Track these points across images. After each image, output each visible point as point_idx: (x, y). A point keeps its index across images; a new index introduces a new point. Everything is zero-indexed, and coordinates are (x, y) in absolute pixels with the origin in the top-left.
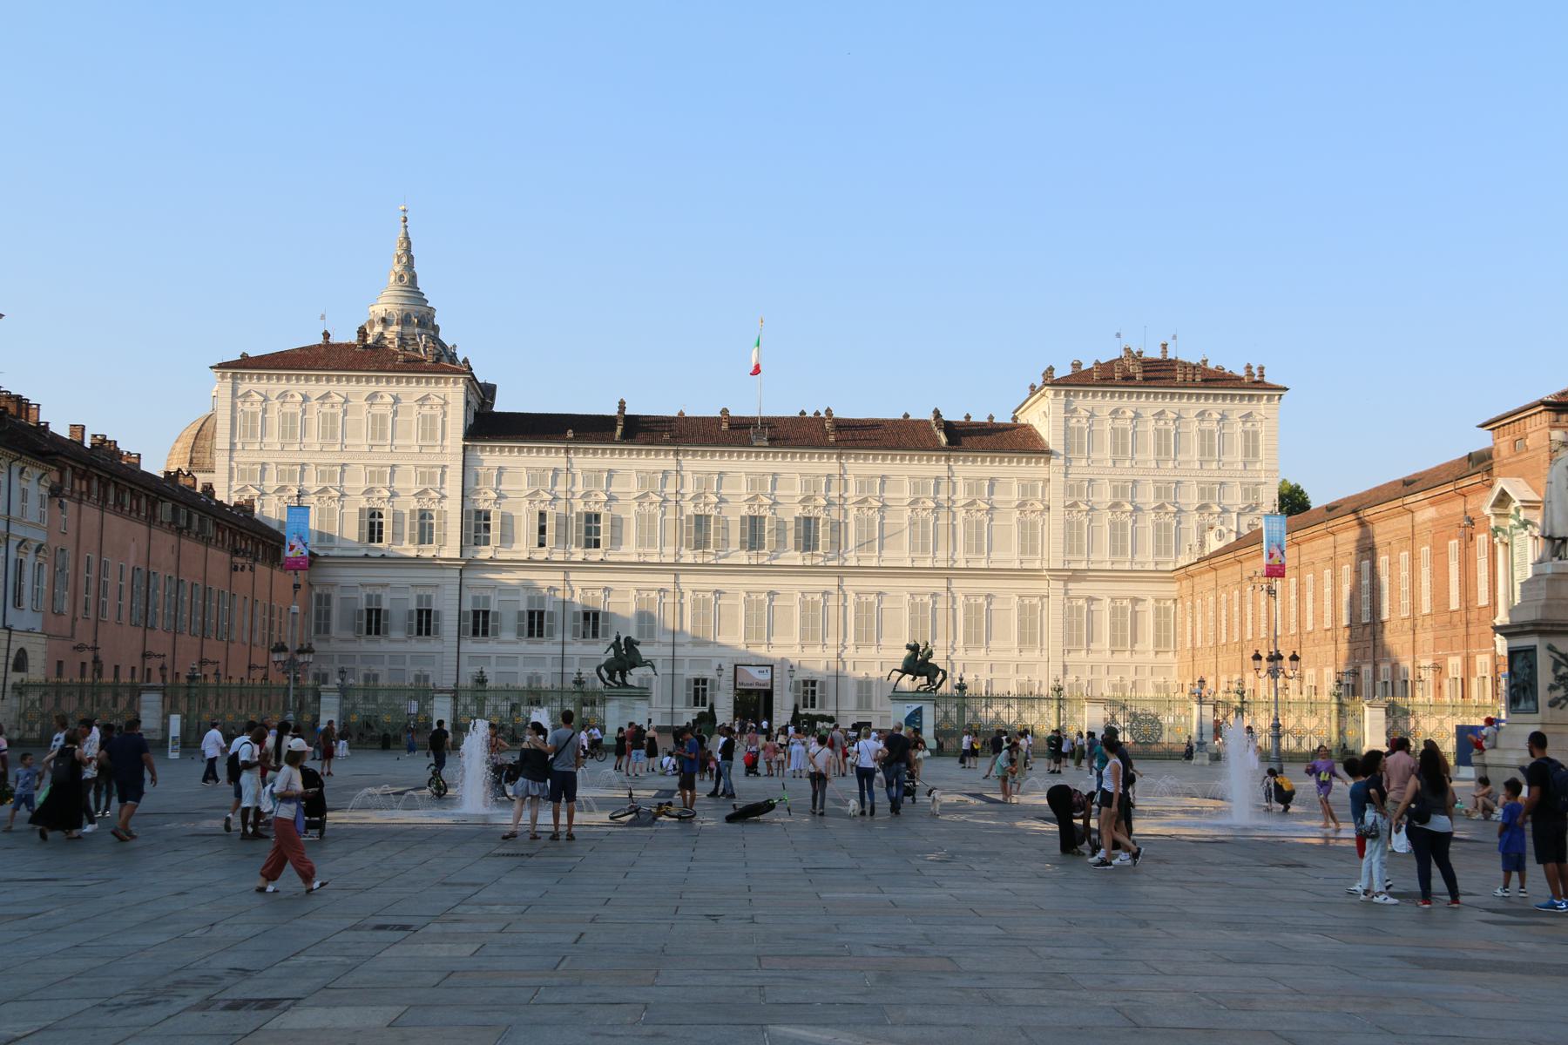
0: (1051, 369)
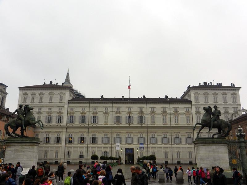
0: (190, 86)
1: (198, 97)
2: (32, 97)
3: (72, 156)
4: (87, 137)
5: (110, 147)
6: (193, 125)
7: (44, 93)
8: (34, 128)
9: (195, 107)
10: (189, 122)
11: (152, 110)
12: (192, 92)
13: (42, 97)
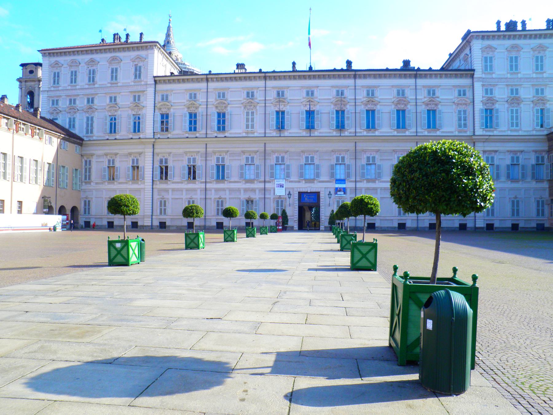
1: (491, 58)
2: (72, 72)
3: (169, 211)
4: (203, 163)
5: (260, 190)
6: (474, 132)
7: (98, 59)
8: (79, 147)
9: (483, 85)
10: (465, 125)
11: (368, 94)
12: (477, 45)
13: (94, 71)
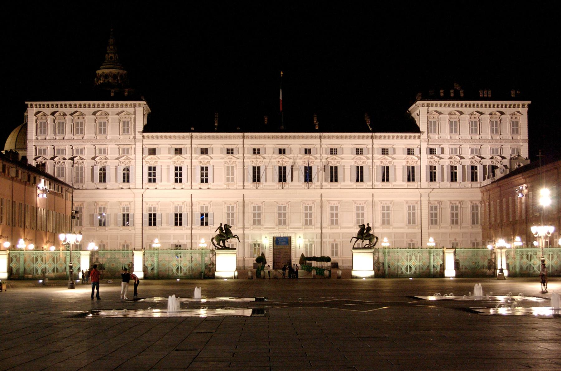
1: (435, 122)
